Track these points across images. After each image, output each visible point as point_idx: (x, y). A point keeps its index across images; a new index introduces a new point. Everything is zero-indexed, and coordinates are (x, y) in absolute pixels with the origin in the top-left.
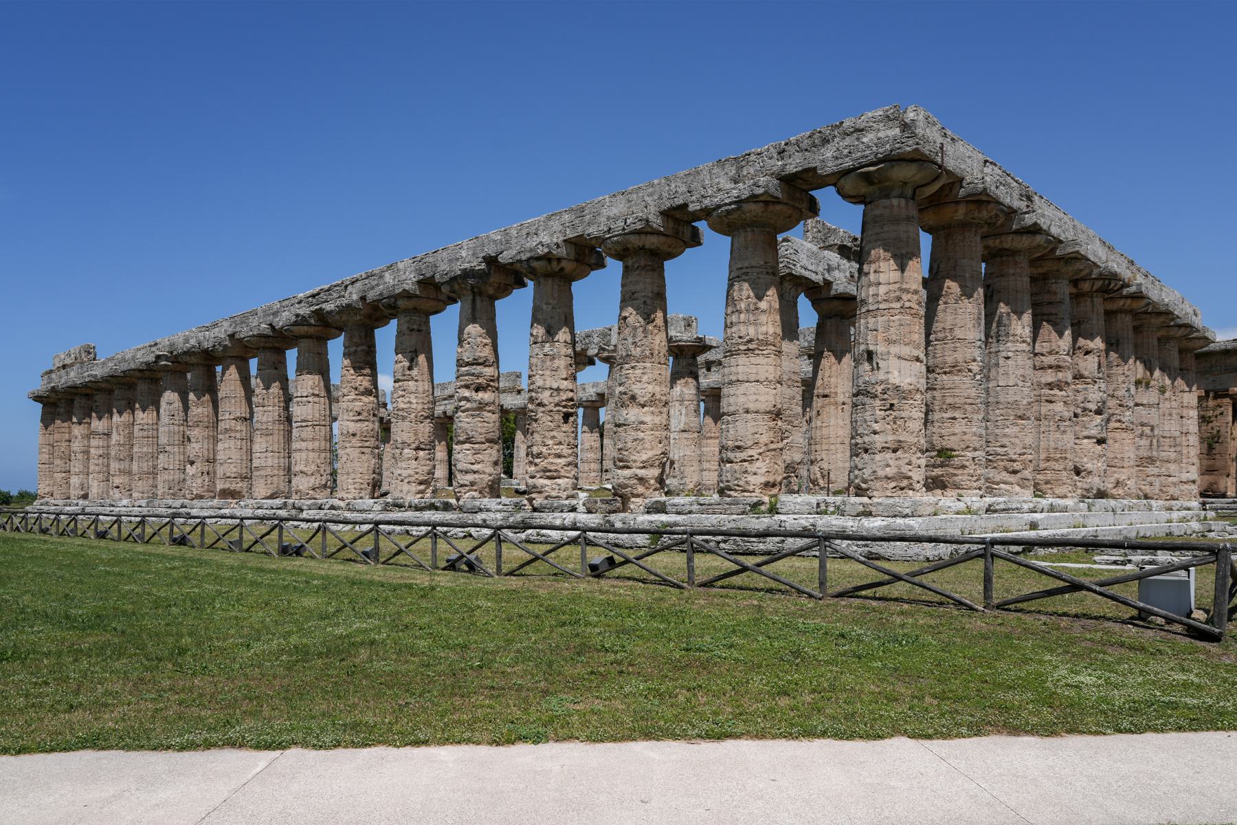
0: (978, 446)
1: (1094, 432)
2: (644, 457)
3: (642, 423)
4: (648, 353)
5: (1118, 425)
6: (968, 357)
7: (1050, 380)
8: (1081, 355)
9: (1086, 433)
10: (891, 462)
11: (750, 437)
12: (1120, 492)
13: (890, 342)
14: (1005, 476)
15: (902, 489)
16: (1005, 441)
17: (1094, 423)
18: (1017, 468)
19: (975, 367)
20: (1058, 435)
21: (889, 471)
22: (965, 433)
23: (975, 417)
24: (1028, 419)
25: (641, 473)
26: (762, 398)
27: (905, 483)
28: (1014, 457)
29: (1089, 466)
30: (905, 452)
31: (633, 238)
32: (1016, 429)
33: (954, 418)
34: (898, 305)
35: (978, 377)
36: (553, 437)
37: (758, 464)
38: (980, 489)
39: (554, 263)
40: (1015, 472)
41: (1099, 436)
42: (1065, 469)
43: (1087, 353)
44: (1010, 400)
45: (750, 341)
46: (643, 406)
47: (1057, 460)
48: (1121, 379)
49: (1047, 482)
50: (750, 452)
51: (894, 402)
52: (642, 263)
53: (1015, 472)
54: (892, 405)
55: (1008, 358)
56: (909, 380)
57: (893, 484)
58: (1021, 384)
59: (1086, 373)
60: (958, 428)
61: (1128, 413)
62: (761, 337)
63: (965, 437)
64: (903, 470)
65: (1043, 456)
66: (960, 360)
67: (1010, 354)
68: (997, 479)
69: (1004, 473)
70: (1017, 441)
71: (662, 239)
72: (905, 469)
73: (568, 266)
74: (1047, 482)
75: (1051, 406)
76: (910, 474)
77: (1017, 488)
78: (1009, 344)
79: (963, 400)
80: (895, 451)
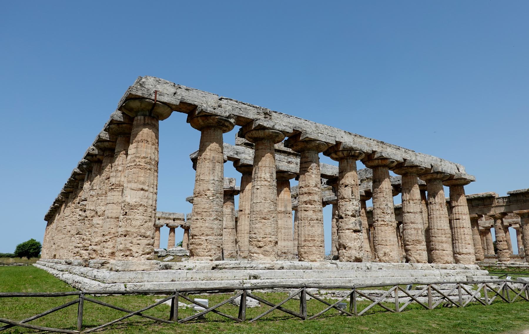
0: (209, 233)
1: (351, 226)
2: (97, 240)
3: (98, 224)
4: (104, 192)
5: (383, 223)
6: (205, 188)
7: (305, 200)
8: (343, 187)
9: (347, 227)
10: (122, 242)
11: (107, 230)
12: (387, 258)
13: (129, 182)
14: (256, 249)
15: (127, 256)
16: (256, 231)
17: (351, 222)
18: (261, 245)
19: (209, 193)
20: (310, 228)
21: (121, 247)
22: (202, 227)
23: (208, 218)
24: (268, 219)
25: (95, 247)
26: (114, 211)
27: (128, 253)
28: (260, 239)
29: (349, 244)
30: (130, 236)
31: (99, 143)
32: (261, 225)
33: (197, 219)
34: (133, 164)
35: (211, 198)
36: (89, 231)
37: (109, 243)
38: (210, 256)
39: (94, 157)
40: (260, 247)
41: (354, 229)
42: (314, 246)
43: (346, 186)
44: (258, 210)
45: (113, 185)
46: (99, 216)
47: (309, 241)
48: (382, 199)
49: (305, 253)
50: (107, 237)
51: (127, 211)
52: (107, 154)
53: (260, 247)
54: (126, 212)
55: (258, 189)
56: (135, 200)
57: (123, 254)
58: (263, 201)
59: (346, 196)
60: (199, 224)
61: (387, 217)
62: (117, 183)
63: (201, 229)
64: (127, 246)
65: (303, 239)
66: (201, 190)
67: (258, 187)
68: (253, 251)
69: (256, 248)
70: (261, 231)
71: (110, 143)
72: (129, 245)
73: (100, 157)
74: (305, 253)
75: (306, 213)
76: (131, 248)
77: (261, 256)
78: (259, 182)
79: (201, 210)
80: (125, 236)
